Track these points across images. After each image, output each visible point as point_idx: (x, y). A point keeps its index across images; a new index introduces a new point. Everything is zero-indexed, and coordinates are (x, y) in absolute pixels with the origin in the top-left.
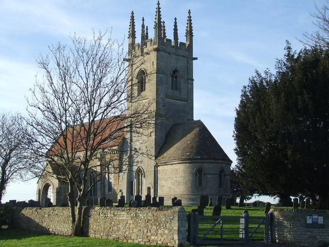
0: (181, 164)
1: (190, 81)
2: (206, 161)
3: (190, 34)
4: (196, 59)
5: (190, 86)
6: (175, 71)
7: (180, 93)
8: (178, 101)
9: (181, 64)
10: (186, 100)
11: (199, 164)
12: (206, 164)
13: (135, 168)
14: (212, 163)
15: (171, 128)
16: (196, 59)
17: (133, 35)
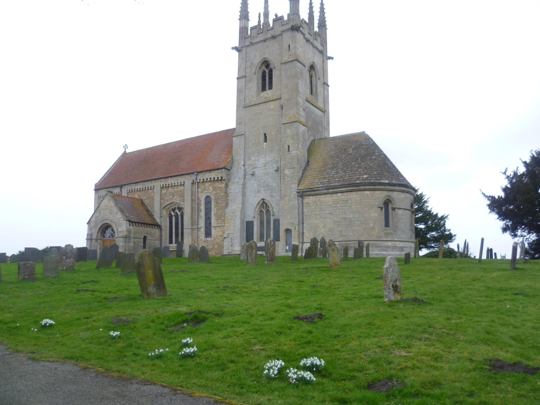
0: (355, 193)
1: (326, 86)
2: (396, 188)
3: (323, 24)
4: (332, 58)
5: (326, 92)
6: (312, 67)
7: (317, 99)
8: (316, 109)
9: (318, 60)
10: (324, 112)
11: (386, 192)
12: (395, 193)
13: (253, 201)
14: (403, 192)
15: (311, 144)
16: (332, 58)
17: (244, 15)
